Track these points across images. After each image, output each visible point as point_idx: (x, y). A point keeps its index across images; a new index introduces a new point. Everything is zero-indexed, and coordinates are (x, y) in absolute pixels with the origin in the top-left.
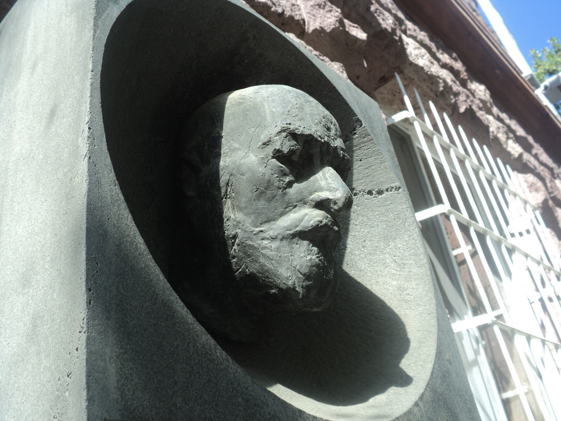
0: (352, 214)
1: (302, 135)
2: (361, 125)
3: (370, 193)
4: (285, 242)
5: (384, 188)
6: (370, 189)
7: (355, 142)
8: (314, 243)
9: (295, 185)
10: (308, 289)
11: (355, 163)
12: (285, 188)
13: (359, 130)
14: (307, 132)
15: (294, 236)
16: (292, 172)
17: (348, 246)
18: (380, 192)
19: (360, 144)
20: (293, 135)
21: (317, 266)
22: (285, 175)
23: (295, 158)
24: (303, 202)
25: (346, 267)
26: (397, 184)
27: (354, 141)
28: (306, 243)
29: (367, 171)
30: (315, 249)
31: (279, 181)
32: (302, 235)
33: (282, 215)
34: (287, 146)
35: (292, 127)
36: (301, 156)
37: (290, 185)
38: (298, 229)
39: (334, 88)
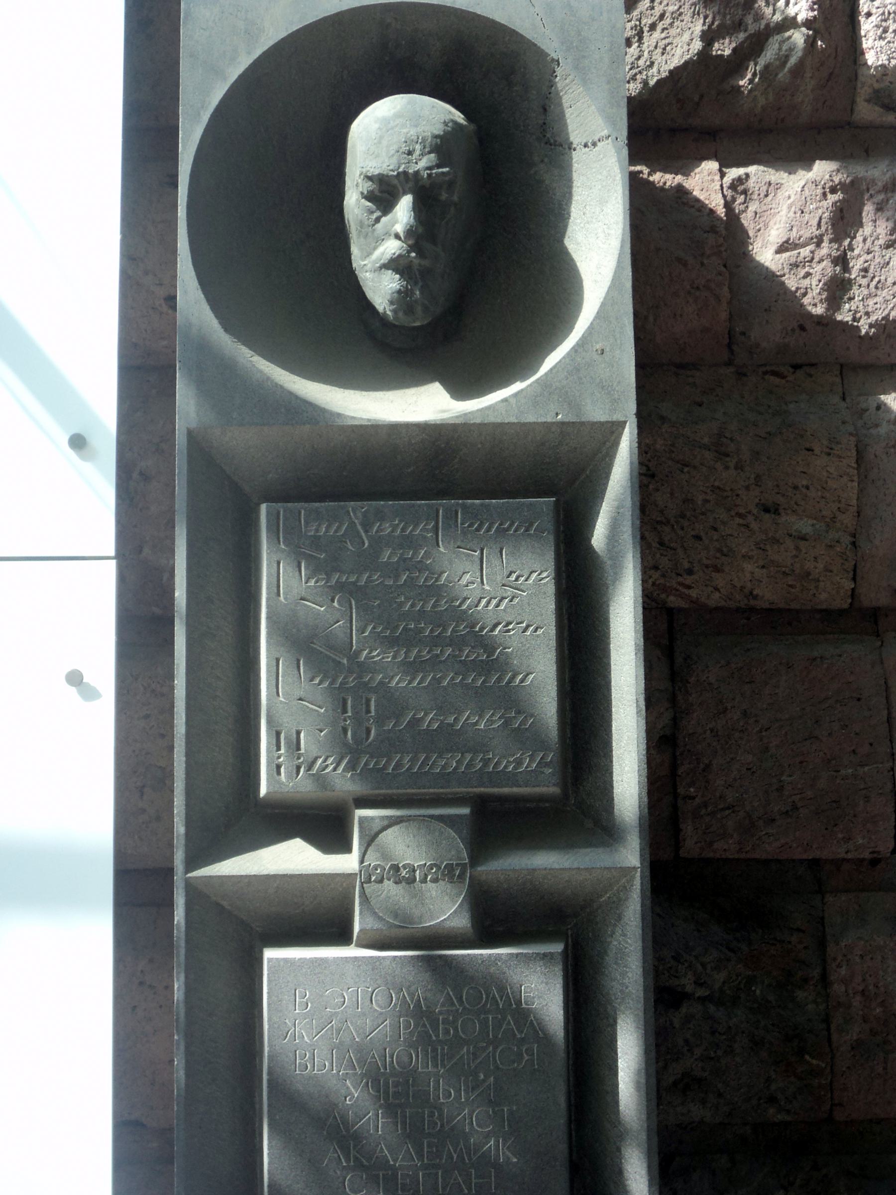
0: (574, 174)
1: (373, 176)
2: (559, 64)
3: (586, 146)
4: (376, 273)
5: (596, 139)
6: (585, 141)
7: (560, 85)
8: (396, 271)
9: (384, 219)
10: (395, 311)
11: (566, 111)
12: (373, 225)
13: (559, 71)
14: (377, 172)
15: (381, 268)
16: (378, 209)
17: (572, 214)
18: (594, 144)
19: (564, 88)
20: (369, 178)
21: (399, 292)
22: (372, 212)
23: (377, 193)
24: (387, 234)
25: (567, 242)
26: (605, 132)
27: (559, 85)
28: (390, 272)
29: (578, 119)
30: (398, 276)
31: (368, 219)
32: (385, 266)
33: (375, 248)
34: (367, 186)
35: (364, 170)
36: (381, 192)
37: (378, 220)
38: (382, 262)
39: (514, 31)
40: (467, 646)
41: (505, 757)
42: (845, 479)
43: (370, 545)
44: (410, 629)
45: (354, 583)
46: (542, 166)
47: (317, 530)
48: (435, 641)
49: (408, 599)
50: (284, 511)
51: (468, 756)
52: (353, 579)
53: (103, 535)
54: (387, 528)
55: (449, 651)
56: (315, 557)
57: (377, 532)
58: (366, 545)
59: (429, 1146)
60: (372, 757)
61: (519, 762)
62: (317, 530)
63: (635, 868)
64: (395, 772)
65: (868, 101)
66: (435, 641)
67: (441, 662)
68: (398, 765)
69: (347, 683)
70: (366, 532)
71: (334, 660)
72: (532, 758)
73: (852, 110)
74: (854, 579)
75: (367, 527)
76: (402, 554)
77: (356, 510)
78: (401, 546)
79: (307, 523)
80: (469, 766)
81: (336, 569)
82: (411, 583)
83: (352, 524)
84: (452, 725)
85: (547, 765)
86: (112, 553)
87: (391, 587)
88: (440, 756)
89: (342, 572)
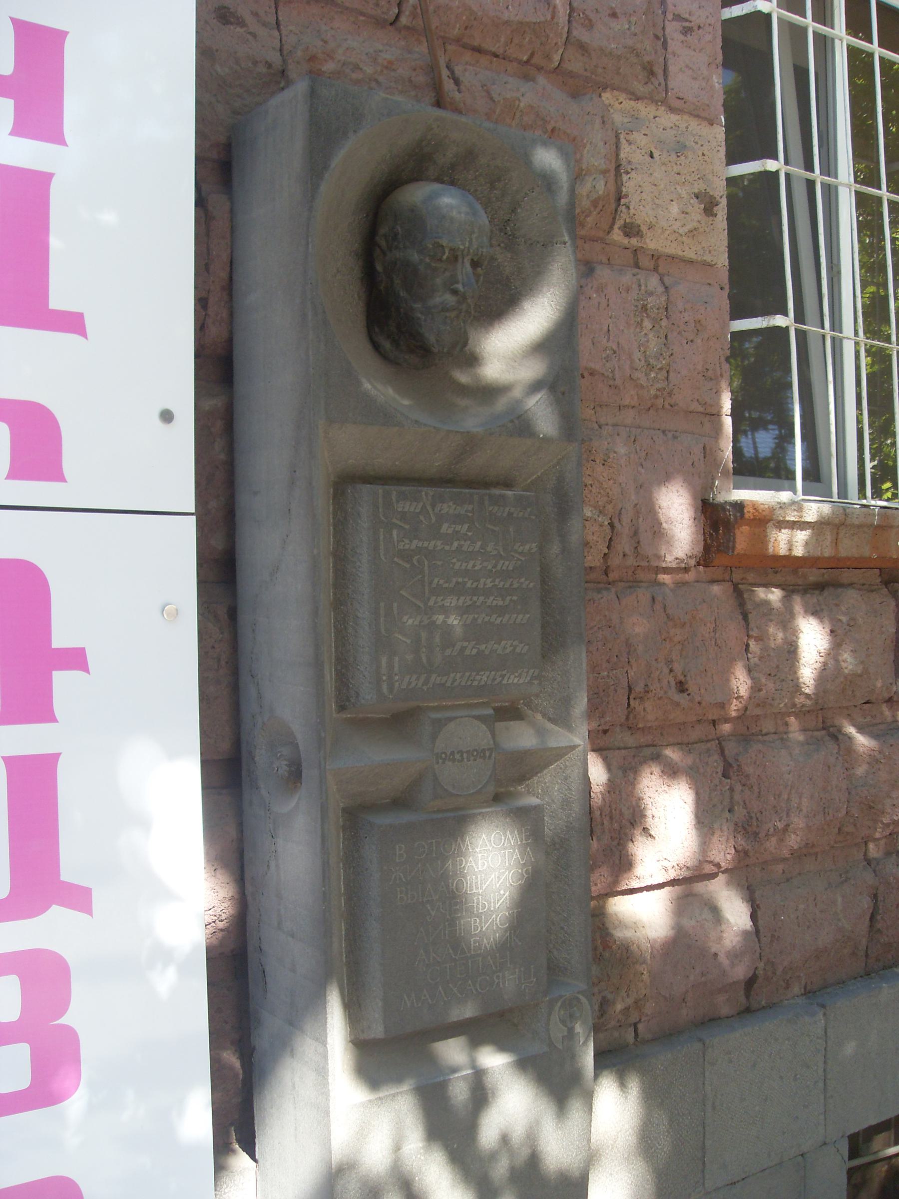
42: (612, 482)
46: (498, 248)
48: (475, 591)
49: (458, 560)
51: (493, 673)
52: (426, 544)
55: (482, 598)
65: (619, 228)
66: (475, 591)
68: (454, 681)
73: (609, 233)
74: (608, 547)
75: (433, 506)
77: (427, 493)
80: (494, 679)
84: (483, 651)
86: (193, 511)
88: (478, 674)
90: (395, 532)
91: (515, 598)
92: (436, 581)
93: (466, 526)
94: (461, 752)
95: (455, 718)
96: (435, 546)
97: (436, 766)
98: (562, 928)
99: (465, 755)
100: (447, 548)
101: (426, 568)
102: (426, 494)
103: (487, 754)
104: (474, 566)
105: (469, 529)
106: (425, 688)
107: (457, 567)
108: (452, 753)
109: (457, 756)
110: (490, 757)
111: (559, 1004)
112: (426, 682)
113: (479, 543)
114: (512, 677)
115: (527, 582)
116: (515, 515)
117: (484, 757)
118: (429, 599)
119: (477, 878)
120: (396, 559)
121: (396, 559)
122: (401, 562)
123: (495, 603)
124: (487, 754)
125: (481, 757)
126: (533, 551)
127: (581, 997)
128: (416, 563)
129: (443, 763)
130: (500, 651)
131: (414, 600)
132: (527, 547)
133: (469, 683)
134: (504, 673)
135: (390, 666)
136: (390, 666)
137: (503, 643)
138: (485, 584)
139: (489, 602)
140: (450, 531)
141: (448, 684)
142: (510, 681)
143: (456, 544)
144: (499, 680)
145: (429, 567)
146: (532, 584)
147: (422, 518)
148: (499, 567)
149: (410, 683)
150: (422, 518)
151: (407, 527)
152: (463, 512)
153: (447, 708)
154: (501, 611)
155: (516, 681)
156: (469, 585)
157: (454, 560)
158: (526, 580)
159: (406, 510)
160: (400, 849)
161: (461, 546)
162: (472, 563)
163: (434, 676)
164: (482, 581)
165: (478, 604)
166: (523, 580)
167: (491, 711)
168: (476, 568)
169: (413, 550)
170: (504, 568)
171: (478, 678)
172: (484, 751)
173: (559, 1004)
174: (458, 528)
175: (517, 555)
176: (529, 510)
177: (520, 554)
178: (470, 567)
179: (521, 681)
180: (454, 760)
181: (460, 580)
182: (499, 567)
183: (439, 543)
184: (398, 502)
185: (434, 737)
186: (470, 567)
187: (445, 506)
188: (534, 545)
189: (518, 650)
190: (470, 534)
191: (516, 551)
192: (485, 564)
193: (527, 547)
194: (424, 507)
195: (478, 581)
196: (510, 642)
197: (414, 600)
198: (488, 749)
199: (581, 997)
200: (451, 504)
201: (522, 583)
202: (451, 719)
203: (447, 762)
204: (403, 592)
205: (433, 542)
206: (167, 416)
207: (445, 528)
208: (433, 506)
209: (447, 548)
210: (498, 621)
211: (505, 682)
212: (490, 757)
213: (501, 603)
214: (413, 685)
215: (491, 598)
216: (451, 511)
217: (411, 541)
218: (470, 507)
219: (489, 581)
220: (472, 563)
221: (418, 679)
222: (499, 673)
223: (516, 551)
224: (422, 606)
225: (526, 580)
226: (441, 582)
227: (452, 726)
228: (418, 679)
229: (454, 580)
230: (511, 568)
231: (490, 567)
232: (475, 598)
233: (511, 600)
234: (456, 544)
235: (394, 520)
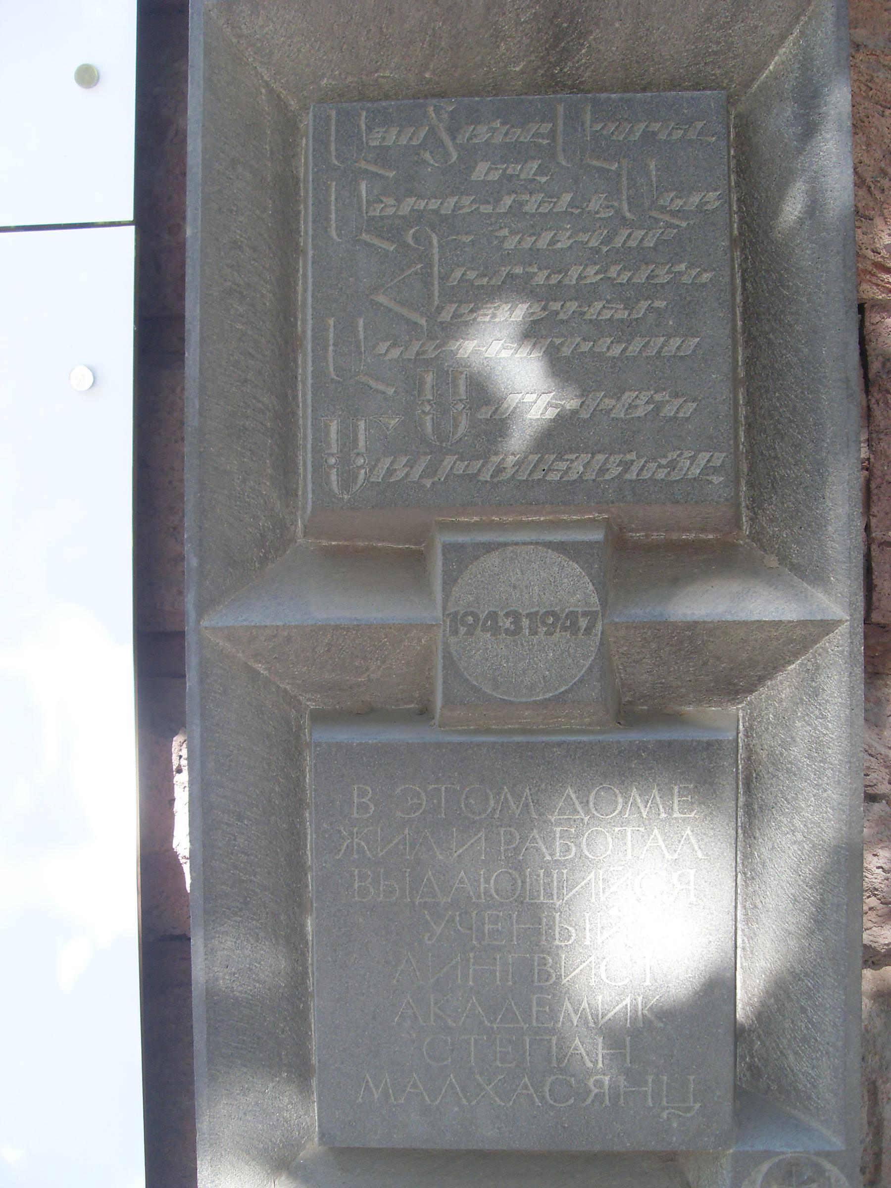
40: (600, 299)
41: (654, 460)
43: (460, 158)
44: (517, 276)
45: (436, 212)
47: (383, 139)
49: (513, 232)
50: (338, 114)
51: (601, 457)
52: (434, 204)
53: (111, 184)
54: (483, 133)
55: (573, 306)
56: (382, 177)
57: (470, 138)
58: (455, 156)
59: (539, 1004)
60: (461, 459)
61: (672, 465)
62: (383, 139)
63: (840, 622)
64: (496, 480)
67: (562, 322)
69: (424, 352)
70: (454, 138)
71: (408, 321)
72: (693, 459)
75: (453, 132)
76: (505, 170)
78: (504, 159)
79: (369, 129)
80: (602, 471)
81: (410, 193)
82: (517, 210)
83: (432, 131)
85: (716, 471)
86: (131, 218)
87: (489, 216)
88: (560, 458)
89: (421, 197)
90: (363, 186)
91: (660, 304)
92: (458, 273)
93: (535, 165)
94: (516, 617)
95: (505, 545)
96: (457, 207)
97: (453, 640)
98: (803, 1010)
99: (525, 623)
100: (486, 209)
101: (435, 250)
102: (437, 110)
103: (583, 623)
104: (553, 242)
105: (541, 171)
106: (428, 483)
107: (511, 244)
108: (493, 616)
109: (507, 623)
110: (588, 631)
111: (765, 1167)
112: (431, 470)
113: (567, 197)
114: (653, 465)
115: (694, 273)
116: (662, 137)
117: (573, 628)
118: (439, 309)
119: (548, 874)
120: (365, 236)
121: (365, 236)
122: (376, 241)
123: (607, 315)
124: (583, 623)
125: (565, 628)
126: (708, 207)
127: (827, 1165)
128: (411, 242)
129: (470, 633)
130: (619, 413)
131: (404, 311)
132: (695, 199)
133: (538, 475)
134: (629, 457)
135: (348, 440)
136: (348, 440)
137: (628, 397)
138: (580, 278)
139: (591, 313)
140: (495, 176)
141: (486, 476)
142: (646, 475)
143: (508, 201)
144: (615, 471)
145: (441, 247)
146: (706, 277)
147: (427, 156)
148: (618, 242)
149: (390, 472)
150: (427, 156)
151: (391, 174)
152: (526, 138)
153: (480, 527)
154: (626, 330)
155: (661, 474)
156: (540, 279)
157: (505, 232)
158: (690, 266)
159: (389, 143)
160: (363, 793)
161: (522, 204)
162: (547, 236)
163: (449, 460)
164: (574, 272)
165: (562, 316)
166: (682, 267)
167: (597, 536)
168: (559, 245)
169: (403, 217)
170: (633, 244)
171: (563, 466)
172: (573, 616)
173: (765, 1167)
174: (514, 169)
175: (667, 218)
176: (700, 125)
177: (673, 214)
178: (543, 243)
179: (676, 476)
180: (495, 630)
181: (519, 270)
182: (618, 242)
183: (466, 201)
184: (369, 129)
185: (450, 581)
186: (543, 243)
187: (482, 129)
188: (712, 195)
189: (668, 411)
190: (544, 179)
191: (663, 209)
192: (583, 237)
193: (695, 199)
194: (432, 131)
195: (564, 271)
196: (644, 396)
197: (404, 311)
198: (585, 614)
199: (827, 1165)
200: (497, 124)
201: (681, 274)
202: (489, 548)
203: (478, 631)
204: (381, 299)
205: (452, 201)
206: (87, 76)
207: (481, 171)
208: (453, 132)
209: (486, 209)
210: (616, 351)
211: (632, 475)
212: (588, 631)
213: (623, 314)
214: (400, 475)
215: (598, 305)
216: (498, 139)
217: (399, 201)
218: (546, 128)
219: (591, 270)
220: (547, 236)
221: (410, 465)
222: (618, 458)
223: (663, 209)
224: (423, 322)
225: (690, 266)
226: (472, 275)
227: (494, 558)
228: (410, 465)
229: (504, 271)
230: (650, 243)
231: (594, 243)
232: (556, 306)
233: (650, 309)
234: (508, 201)
235: (363, 165)
